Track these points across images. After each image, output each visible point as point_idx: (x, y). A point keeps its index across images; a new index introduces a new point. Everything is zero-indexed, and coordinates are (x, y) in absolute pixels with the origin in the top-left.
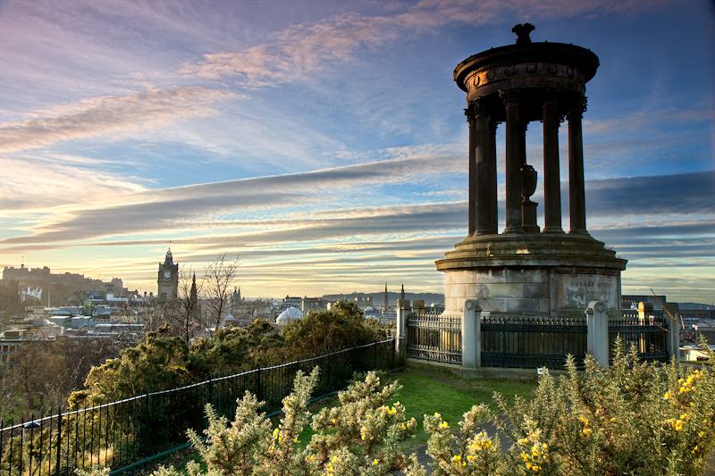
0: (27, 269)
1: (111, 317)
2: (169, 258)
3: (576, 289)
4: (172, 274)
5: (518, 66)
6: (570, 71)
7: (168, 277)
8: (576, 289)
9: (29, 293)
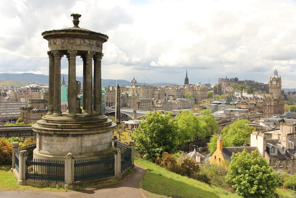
0: (228, 79)
3: (46, 142)
6: (63, 41)
8: (46, 142)
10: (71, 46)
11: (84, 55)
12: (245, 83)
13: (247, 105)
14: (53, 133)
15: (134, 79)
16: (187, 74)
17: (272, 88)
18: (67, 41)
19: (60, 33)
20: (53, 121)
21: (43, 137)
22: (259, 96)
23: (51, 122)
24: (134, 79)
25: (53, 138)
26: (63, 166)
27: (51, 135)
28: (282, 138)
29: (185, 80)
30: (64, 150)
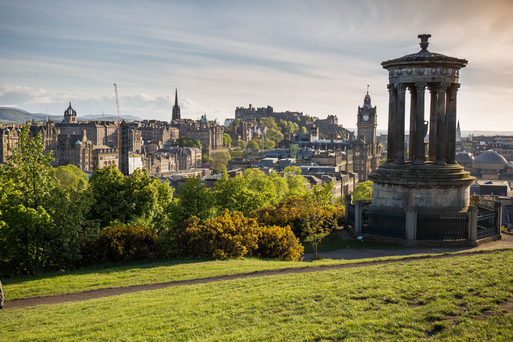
2: (367, 100)
4: (370, 117)
5: (403, 70)
6: (434, 70)
8: (419, 196)
9: (255, 131)
10: (444, 77)
11: (434, 87)
13: (330, 159)
14: (436, 184)
15: (70, 107)
17: (362, 127)
18: (439, 70)
19: (437, 62)
20: (426, 170)
23: (420, 171)
24: (70, 107)
25: (431, 190)
27: (429, 187)
28: (486, 203)
30: (444, 205)
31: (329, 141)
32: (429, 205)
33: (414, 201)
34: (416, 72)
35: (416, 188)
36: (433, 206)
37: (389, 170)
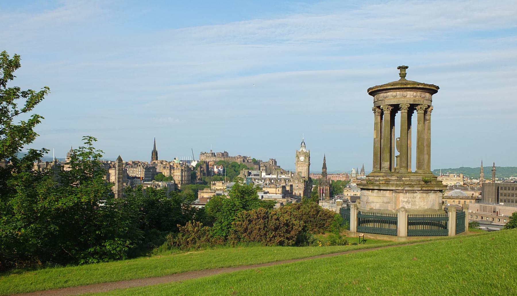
1: (263, 189)
4: (305, 158)
5: (388, 93)
7: (302, 160)
8: (406, 200)
12: (239, 159)
16: (155, 145)
21: (401, 194)
22: (283, 176)
25: (415, 195)
26: (447, 219)
27: (414, 191)
29: (152, 153)
30: (426, 207)
31: (274, 176)
32: (414, 208)
33: (401, 204)
34: (400, 95)
35: (403, 192)
36: (417, 208)
37: (378, 178)
